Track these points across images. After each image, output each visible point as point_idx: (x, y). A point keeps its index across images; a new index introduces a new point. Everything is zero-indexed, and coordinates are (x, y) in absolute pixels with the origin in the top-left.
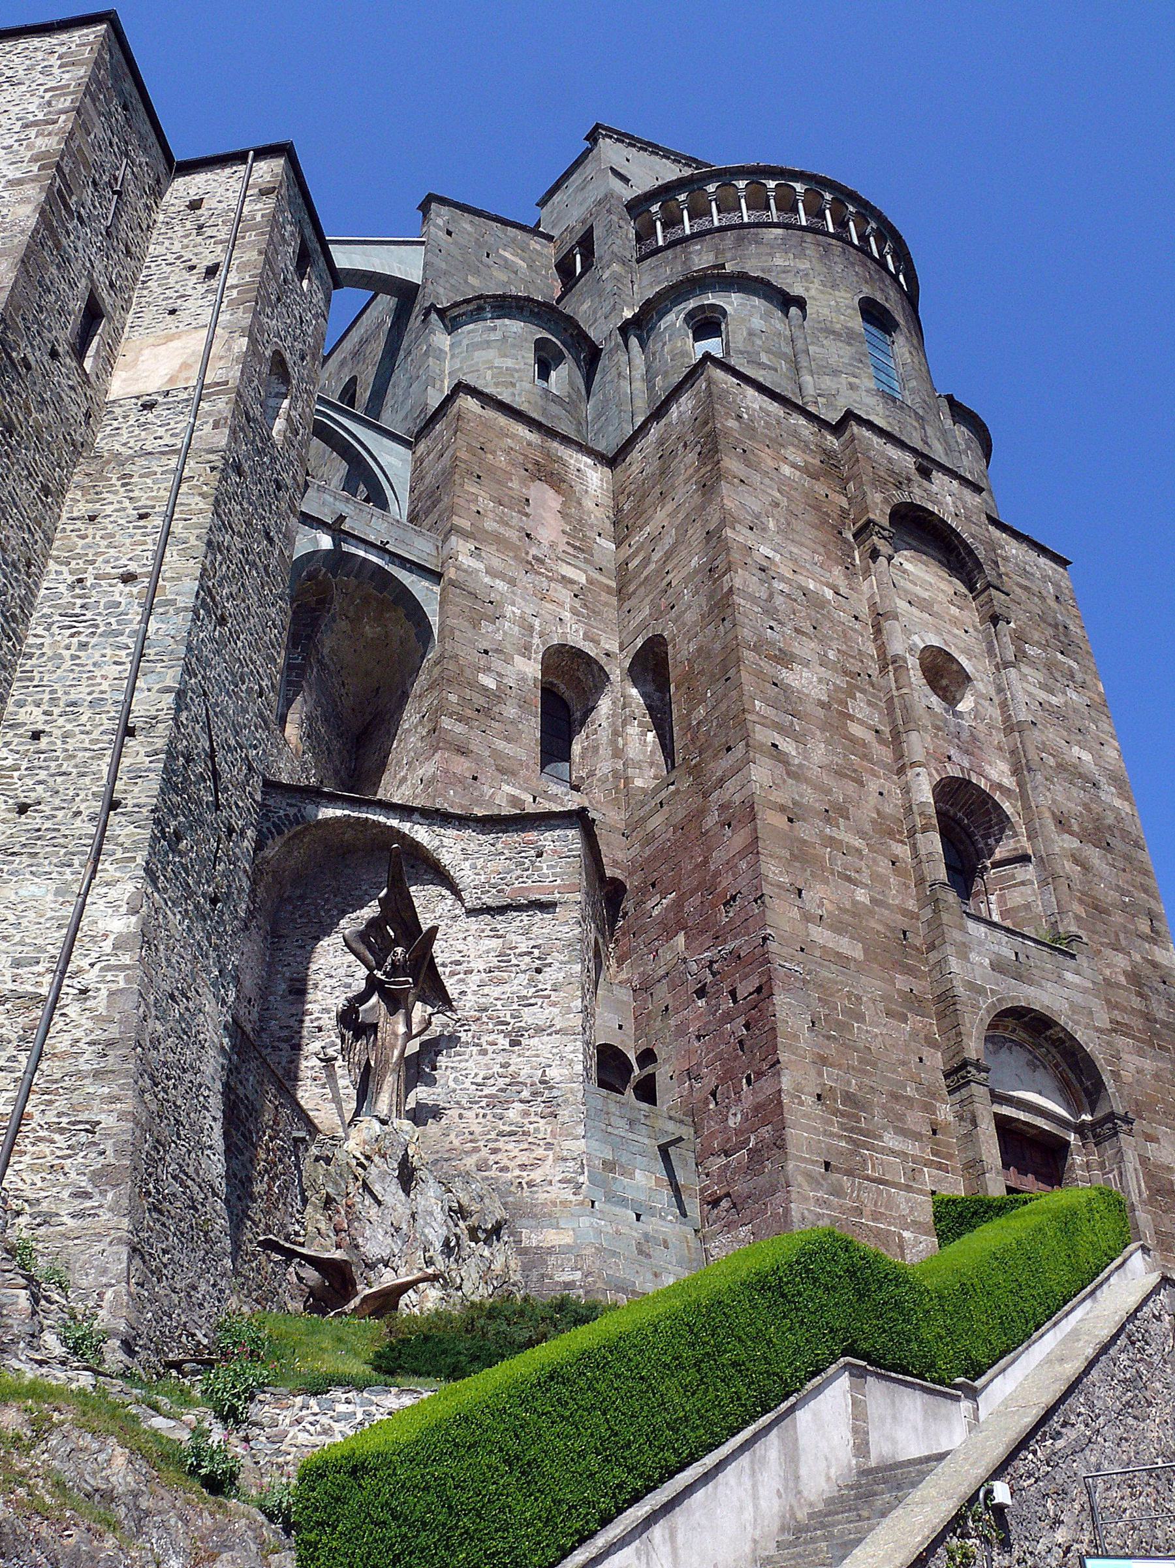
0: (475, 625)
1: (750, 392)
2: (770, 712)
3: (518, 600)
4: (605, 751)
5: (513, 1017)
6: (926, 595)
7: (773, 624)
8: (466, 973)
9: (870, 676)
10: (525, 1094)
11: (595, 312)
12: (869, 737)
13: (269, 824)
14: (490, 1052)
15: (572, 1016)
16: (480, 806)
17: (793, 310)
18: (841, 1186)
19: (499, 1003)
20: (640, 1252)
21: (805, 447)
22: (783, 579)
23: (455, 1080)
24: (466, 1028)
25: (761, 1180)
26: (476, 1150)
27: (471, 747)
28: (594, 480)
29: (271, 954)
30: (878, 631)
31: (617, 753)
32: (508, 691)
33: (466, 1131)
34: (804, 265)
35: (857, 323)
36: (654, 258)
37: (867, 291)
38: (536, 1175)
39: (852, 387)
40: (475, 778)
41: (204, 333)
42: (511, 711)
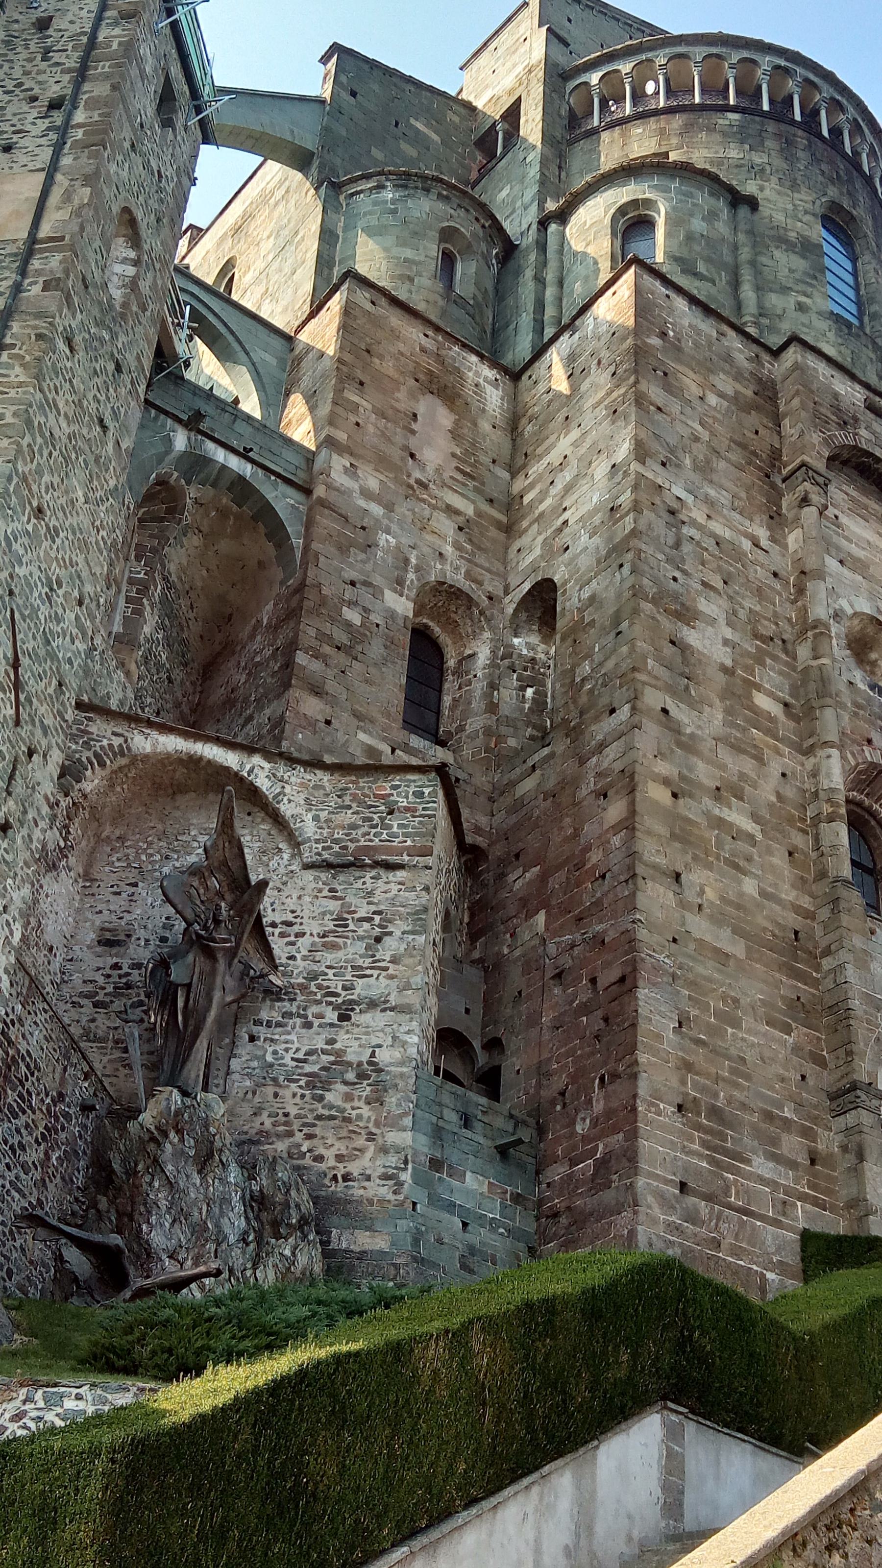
0: (343, 549)
1: (681, 304)
2: (662, 672)
3: (394, 527)
4: (478, 704)
5: (345, 988)
6: (861, 554)
7: (677, 574)
8: (297, 935)
9: (784, 641)
10: (351, 1076)
11: (514, 202)
12: (776, 709)
13: (90, 754)
14: (316, 1024)
15: (410, 992)
16: (331, 752)
17: (743, 211)
18: (697, 1211)
19: (331, 972)
20: (464, 1267)
21: (738, 376)
22: (694, 523)
23: (275, 1052)
25: (608, 1196)
26: (290, 1134)
27: (327, 688)
28: (494, 398)
29: (81, 900)
30: (801, 591)
31: (492, 708)
33: (281, 1112)
34: (759, 159)
35: (818, 233)
36: (589, 140)
37: (833, 192)
38: (354, 1168)
39: (801, 308)
41: (42, 176)
42: (376, 649)
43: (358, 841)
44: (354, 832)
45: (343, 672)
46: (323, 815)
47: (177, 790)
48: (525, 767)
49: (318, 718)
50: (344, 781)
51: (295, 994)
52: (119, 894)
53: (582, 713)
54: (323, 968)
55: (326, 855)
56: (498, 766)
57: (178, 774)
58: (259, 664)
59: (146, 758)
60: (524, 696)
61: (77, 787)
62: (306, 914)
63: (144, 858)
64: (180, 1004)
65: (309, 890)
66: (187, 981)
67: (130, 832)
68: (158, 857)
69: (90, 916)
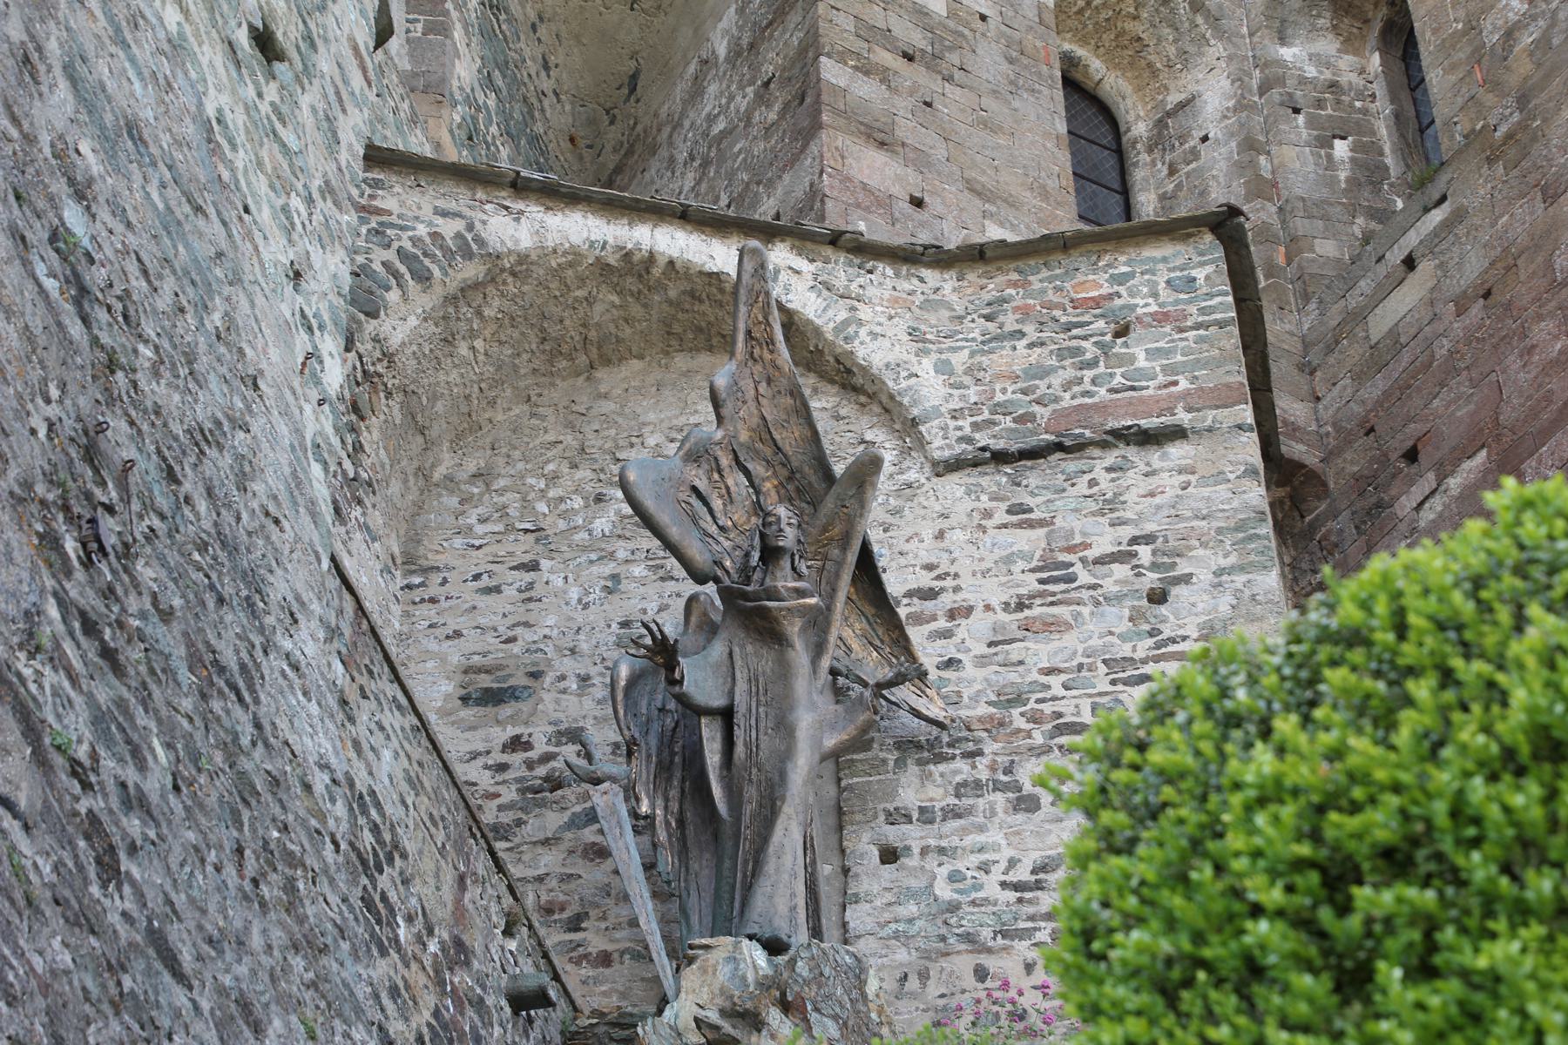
8: (952, 615)
13: (390, 255)
19: (1055, 682)
23: (955, 877)
24: (971, 746)
29: (407, 614)
32: (979, 24)
40: (918, 203)
42: (989, 62)
43: (1057, 400)
44: (1042, 384)
45: (928, 104)
46: (959, 360)
47: (605, 352)
48: (1382, 270)
49: (896, 190)
50: (994, 286)
51: (977, 741)
52: (497, 590)
53: (1523, 100)
54: (1035, 676)
55: (983, 439)
56: (1306, 298)
57: (599, 308)
58: (724, 134)
59: (522, 265)
60: (1330, 157)
61: (370, 326)
62: (964, 566)
63: (542, 507)
64: (713, 757)
65: (959, 517)
66: (718, 702)
67: (501, 461)
68: (577, 502)
69: (433, 646)
